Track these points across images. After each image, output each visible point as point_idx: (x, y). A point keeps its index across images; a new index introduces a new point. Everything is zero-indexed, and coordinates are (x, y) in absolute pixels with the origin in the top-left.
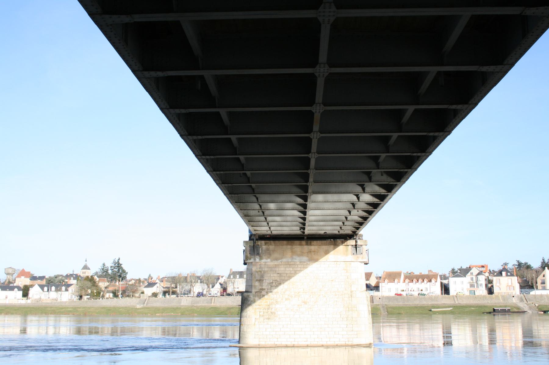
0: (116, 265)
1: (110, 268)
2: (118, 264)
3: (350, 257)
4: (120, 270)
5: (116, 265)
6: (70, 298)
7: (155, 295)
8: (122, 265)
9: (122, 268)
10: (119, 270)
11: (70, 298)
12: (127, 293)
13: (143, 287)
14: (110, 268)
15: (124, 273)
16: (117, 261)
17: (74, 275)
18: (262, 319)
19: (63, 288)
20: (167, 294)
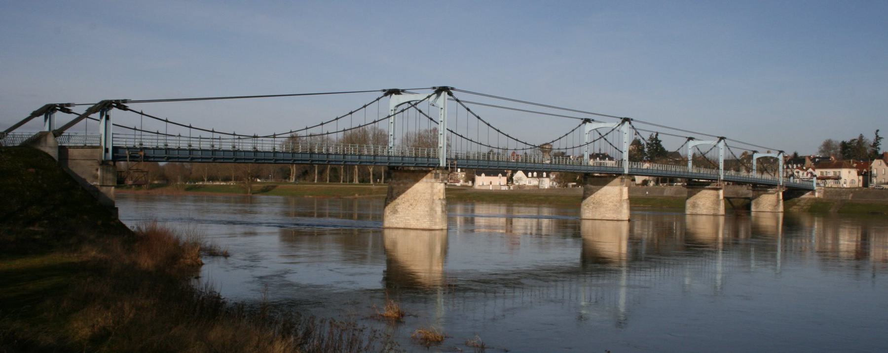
0: (654, 142)
1: (645, 146)
2: (656, 141)
3: (433, 180)
5: (654, 142)
6: (551, 185)
9: (661, 145)
10: (657, 149)
11: (551, 185)
14: (645, 146)
16: (654, 137)
17: (602, 154)
18: (391, 213)
19: (545, 174)
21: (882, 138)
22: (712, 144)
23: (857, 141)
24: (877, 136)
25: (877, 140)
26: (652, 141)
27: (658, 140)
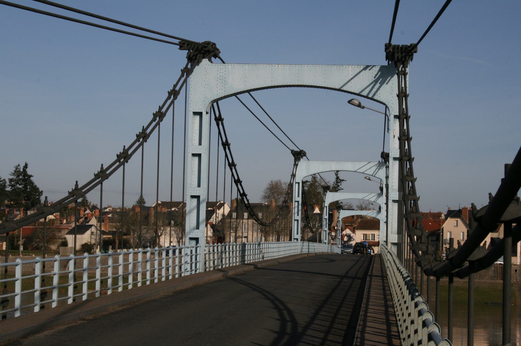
0: (21, 177)
1: (8, 183)
2: (23, 176)
4: (28, 187)
5: (21, 177)
7: (87, 248)
8: (31, 178)
9: (32, 183)
10: (25, 187)
12: (34, 243)
13: (66, 231)
14: (8, 183)
15: (36, 193)
16: (22, 170)
20: (111, 247)
21: (343, 180)
22: (367, 198)
23: (309, 183)
24: (338, 178)
25: (337, 182)
26: (18, 176)
27: (28, 175)
